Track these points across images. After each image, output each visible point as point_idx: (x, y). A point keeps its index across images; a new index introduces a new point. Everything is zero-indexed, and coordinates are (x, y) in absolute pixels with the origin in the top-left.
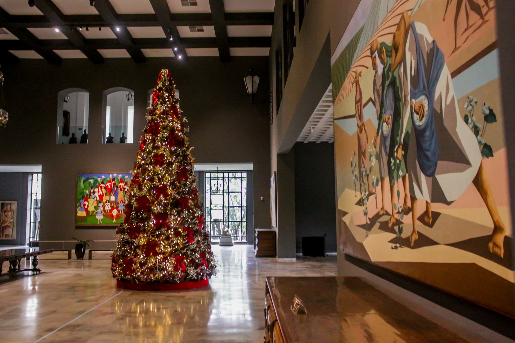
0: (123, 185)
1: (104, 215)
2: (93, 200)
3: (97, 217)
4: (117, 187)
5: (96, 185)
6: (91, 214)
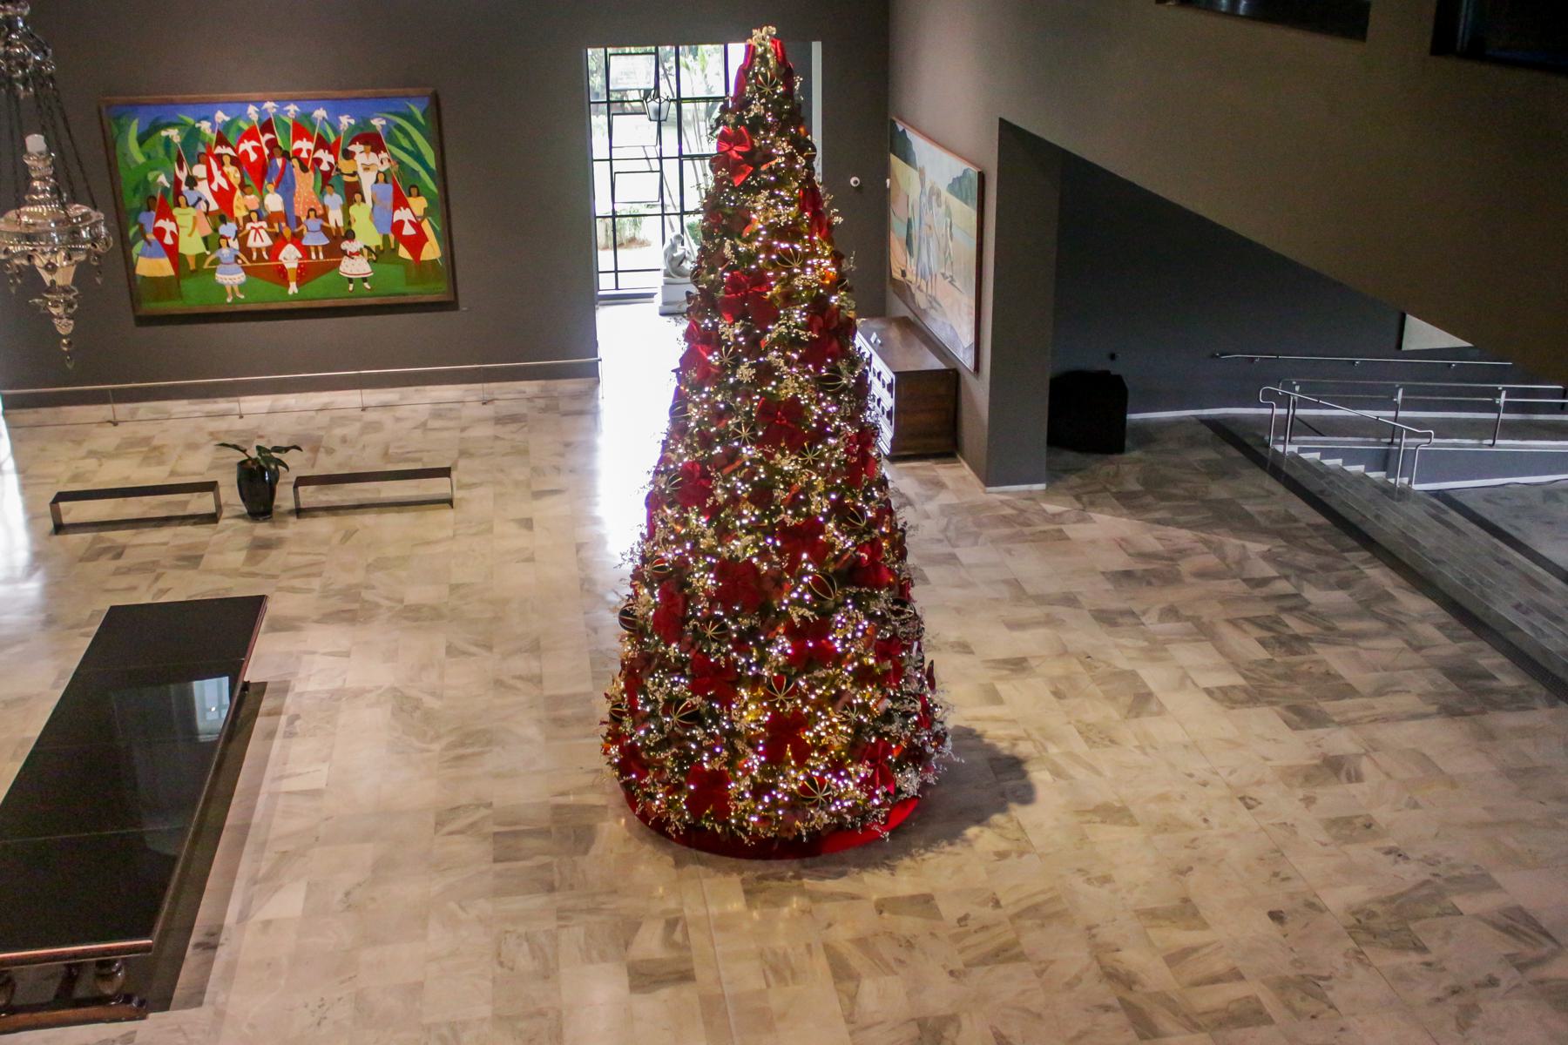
0: (311, 146)
1: (246, 270)
2: (191, 210)
3: (220, 277)
5: (192, 150)
6: (192, 267)
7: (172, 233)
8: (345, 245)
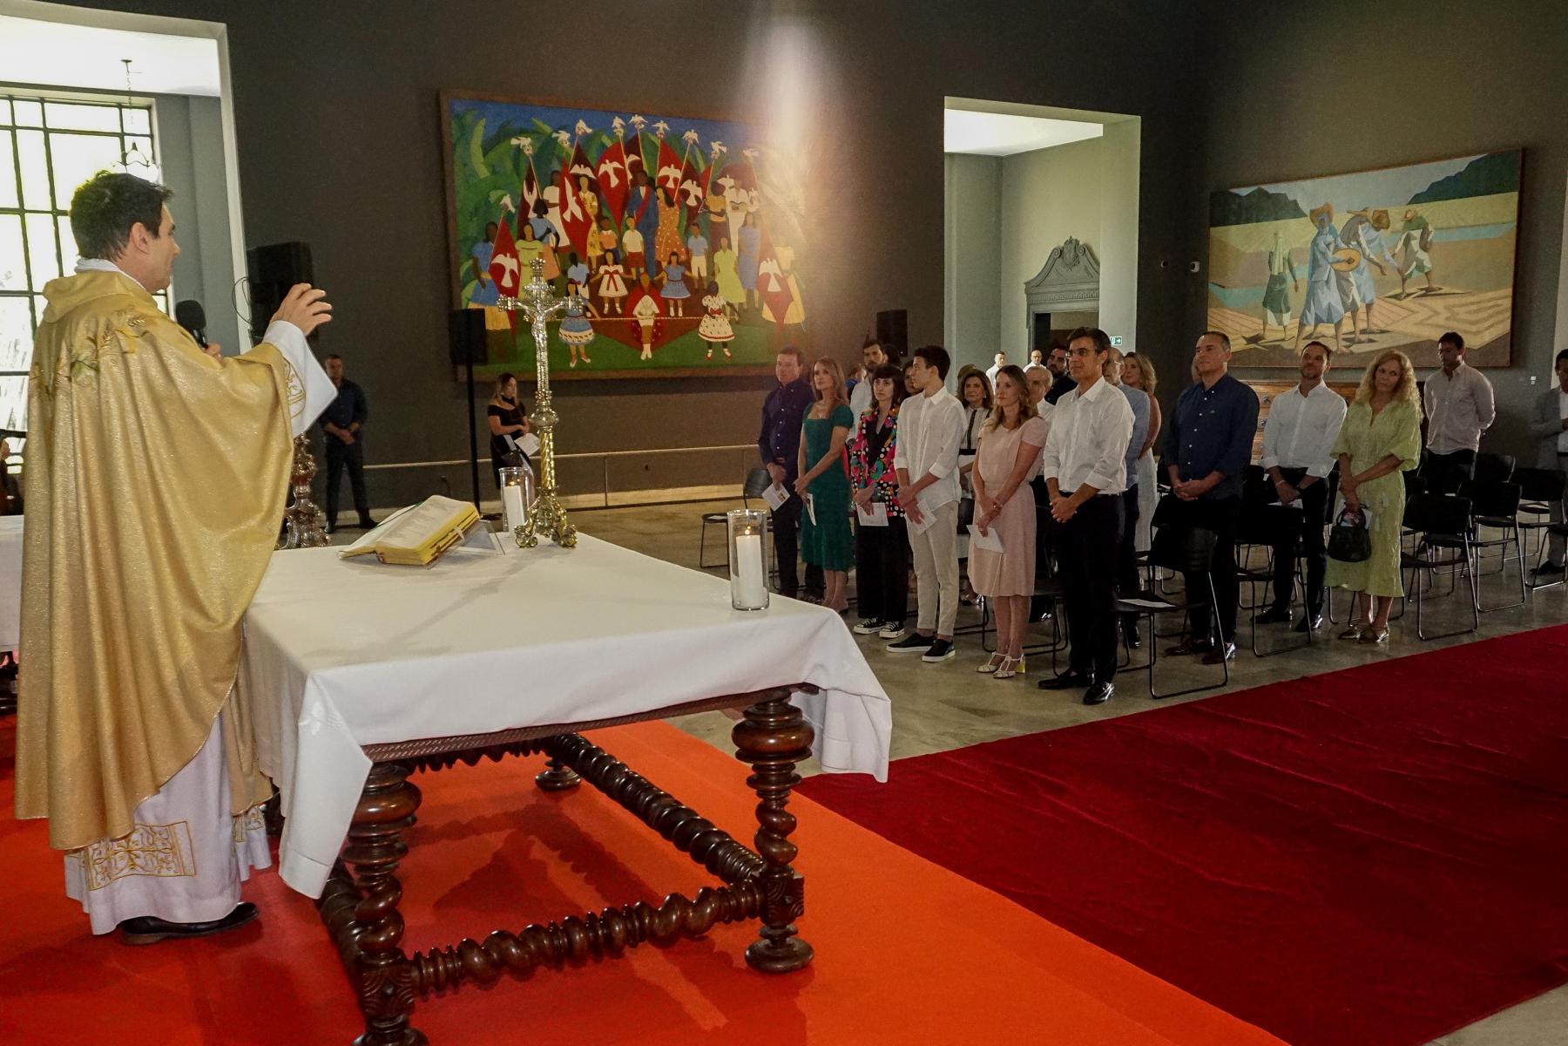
0: (678, 174)
1: (594, 325)
2: (537, 244)
4: (650, 183)
7: (512, 272)
8: (708, 301)
